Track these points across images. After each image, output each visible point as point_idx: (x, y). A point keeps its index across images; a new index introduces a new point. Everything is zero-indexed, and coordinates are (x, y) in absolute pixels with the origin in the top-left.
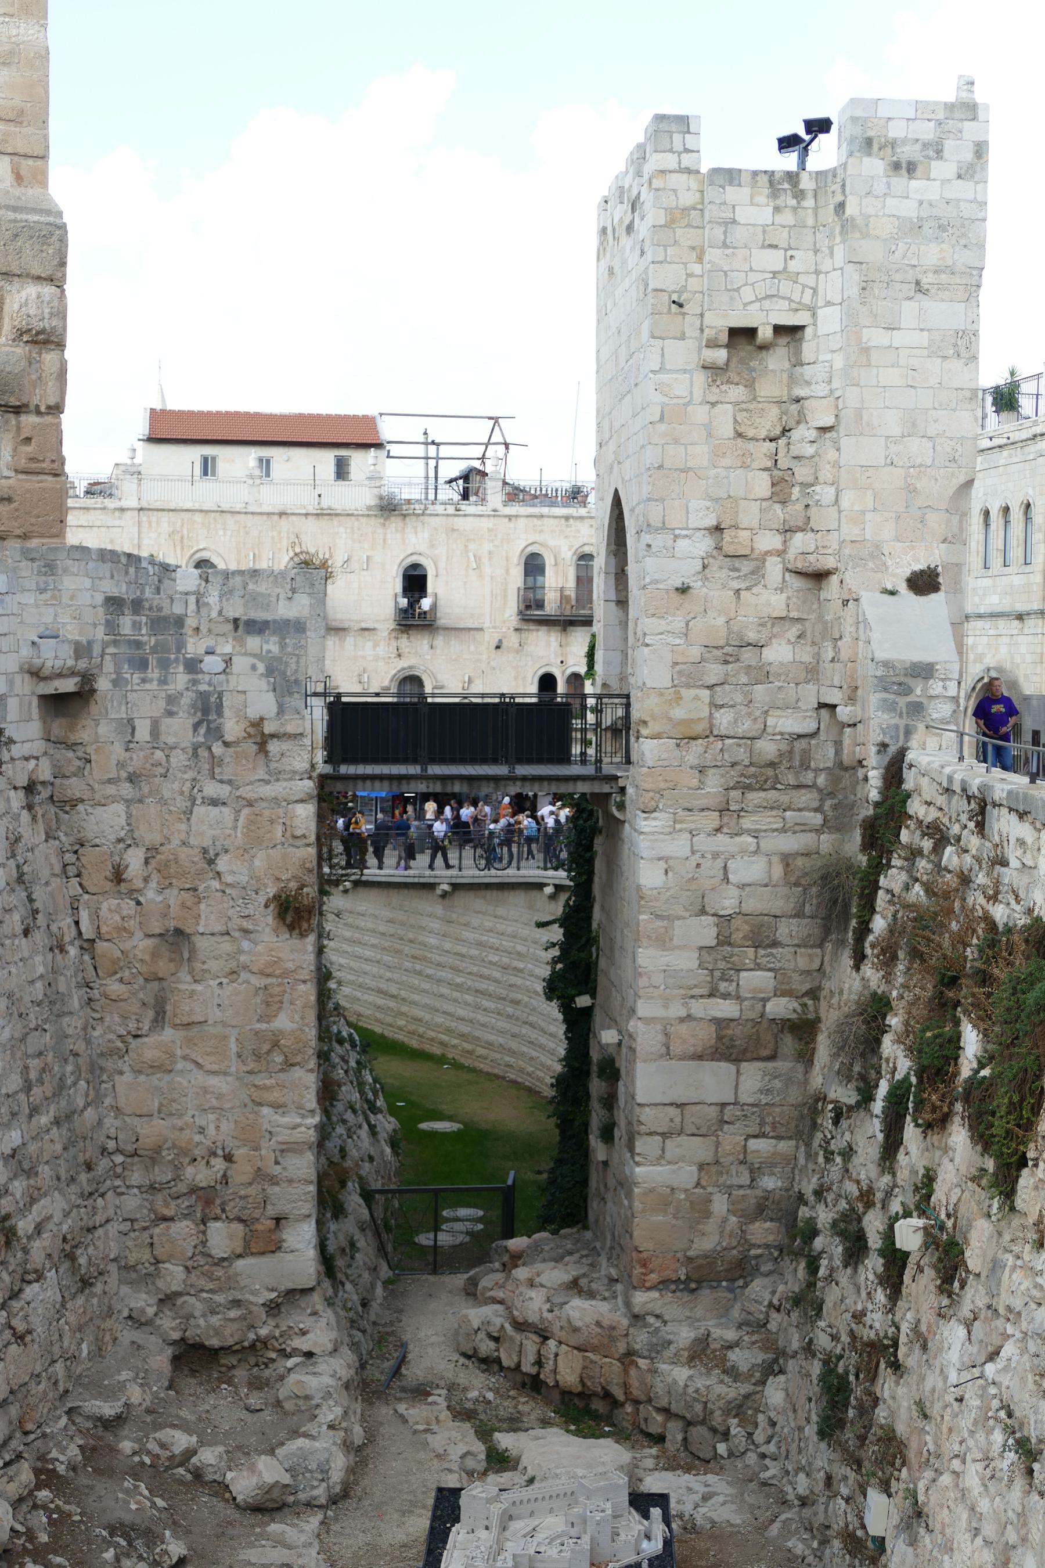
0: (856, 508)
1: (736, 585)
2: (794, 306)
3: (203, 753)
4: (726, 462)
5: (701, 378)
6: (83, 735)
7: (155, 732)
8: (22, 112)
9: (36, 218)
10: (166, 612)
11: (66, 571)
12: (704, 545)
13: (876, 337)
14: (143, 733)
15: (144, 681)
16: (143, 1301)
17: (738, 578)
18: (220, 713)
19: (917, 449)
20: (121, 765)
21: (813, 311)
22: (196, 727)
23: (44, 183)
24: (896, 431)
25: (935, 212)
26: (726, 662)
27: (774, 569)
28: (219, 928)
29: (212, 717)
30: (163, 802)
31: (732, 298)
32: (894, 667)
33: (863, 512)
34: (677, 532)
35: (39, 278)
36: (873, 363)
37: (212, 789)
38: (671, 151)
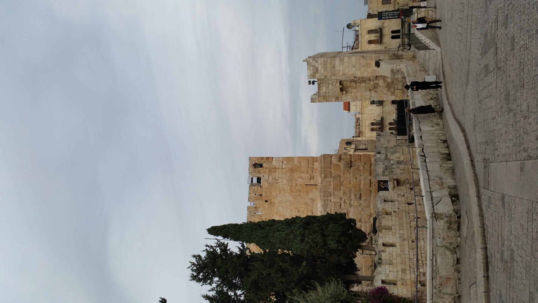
3: (405, 163)
4: (360, 90)
5: (348, 94)
6: (403, 180)
7: (402, 170)
8: (307, 161)
9: (322, 159)
10: (384, 168)
11: (378, 173)
12: (372, 92)
13: (341, 73)
15: (395, 171)
18: (399, 161)
19: (357, 66)
21: (337, 80)
22: (401, 164)
23: (317, 157)
24: (355, 69)
25: (323, 66)
26: (391, 88)
27: (376, 82)
29: (400, 162)
31: (336, 92)
32: (392, 75)
33: (367, 73)
35: (331, 158)
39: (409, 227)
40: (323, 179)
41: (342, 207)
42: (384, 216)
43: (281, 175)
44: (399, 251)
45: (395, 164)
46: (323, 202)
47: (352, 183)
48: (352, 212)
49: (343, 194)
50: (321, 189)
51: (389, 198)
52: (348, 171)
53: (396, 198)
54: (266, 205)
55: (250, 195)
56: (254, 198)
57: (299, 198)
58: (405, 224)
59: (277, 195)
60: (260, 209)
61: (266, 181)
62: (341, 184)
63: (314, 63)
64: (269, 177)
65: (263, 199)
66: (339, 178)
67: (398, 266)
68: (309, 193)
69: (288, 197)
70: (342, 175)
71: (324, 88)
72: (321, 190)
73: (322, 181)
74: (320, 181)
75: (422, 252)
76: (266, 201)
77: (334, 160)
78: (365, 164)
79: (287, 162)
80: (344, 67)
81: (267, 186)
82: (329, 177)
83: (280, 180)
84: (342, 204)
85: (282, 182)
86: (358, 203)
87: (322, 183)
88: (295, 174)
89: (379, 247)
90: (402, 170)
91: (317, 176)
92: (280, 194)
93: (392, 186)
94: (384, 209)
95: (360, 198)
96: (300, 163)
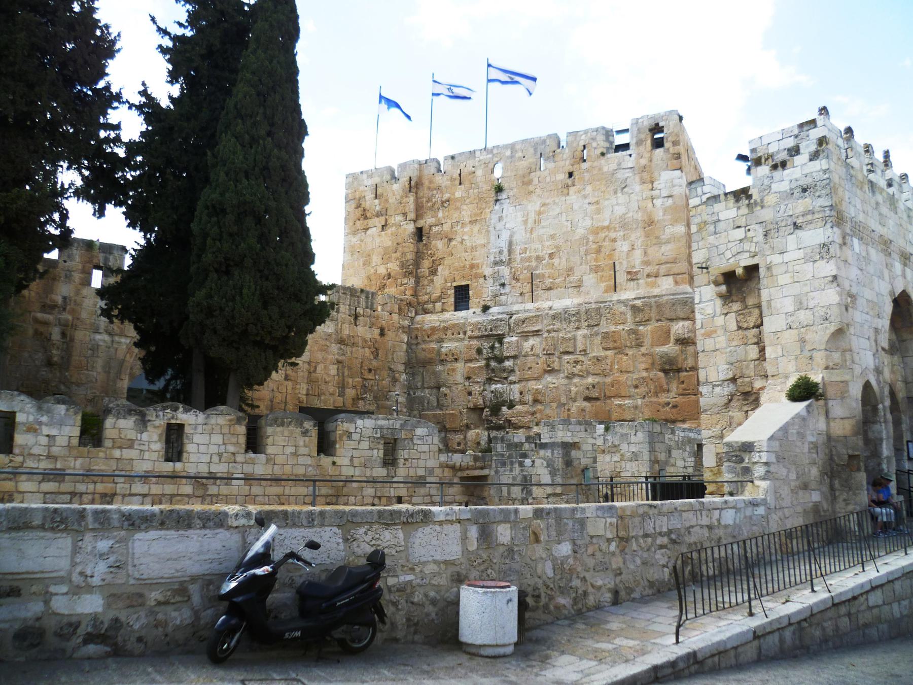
0: (772, 357)
1: (745, 408)
2: (752, 254)
15: (505, 471)
17: (747, 404)
19: (804, 316)
24: (791, 309)
25: (799, 183)
31: (721, 259)
34: (714, 383)
36: (774, 274)
38: (697, 196)
40: (631, 303)
41: (566, 358)
43: (636, 198)
44: (143, 467)
45: (522, 471)
46: (573, 310)
47: (625, 376)
48: (554, 381)
49: (594, 357)
50: (606, 302)
51: (402, 454)
52: (653, 364)
53: (402, 472)
54: (562, 176)
55: (581, 133)
56: (575, 145)
57: (582, 253)
59: (585, 197)
60: (551, 165)
61: (619, 164)
62: (619, 350)
63: (808, 146)
64: (628, 170)
65: (575, 167)
66: (633, 343)
67: (75, 460)
68: (595, 275)
69: (584, 224)
70: (643, 350)
71: (732, 213)
72: (601, 302)
73: (624, 303)
76: (571, 175)
77: (679, 328)
78: (675, 406)
79: (670, 207)
80: (797, 268)
81: (605, 169)
82: (635, 318)
84: (571, 357)
85: (617, 204)
86: (576, 393)
87: (620, 302)
88: (640, 233)
89: (161, 413)
91: (638, 289)
92: (589, 203)
93: (458, 464)
95: (587, 399)
96: (668, 242)
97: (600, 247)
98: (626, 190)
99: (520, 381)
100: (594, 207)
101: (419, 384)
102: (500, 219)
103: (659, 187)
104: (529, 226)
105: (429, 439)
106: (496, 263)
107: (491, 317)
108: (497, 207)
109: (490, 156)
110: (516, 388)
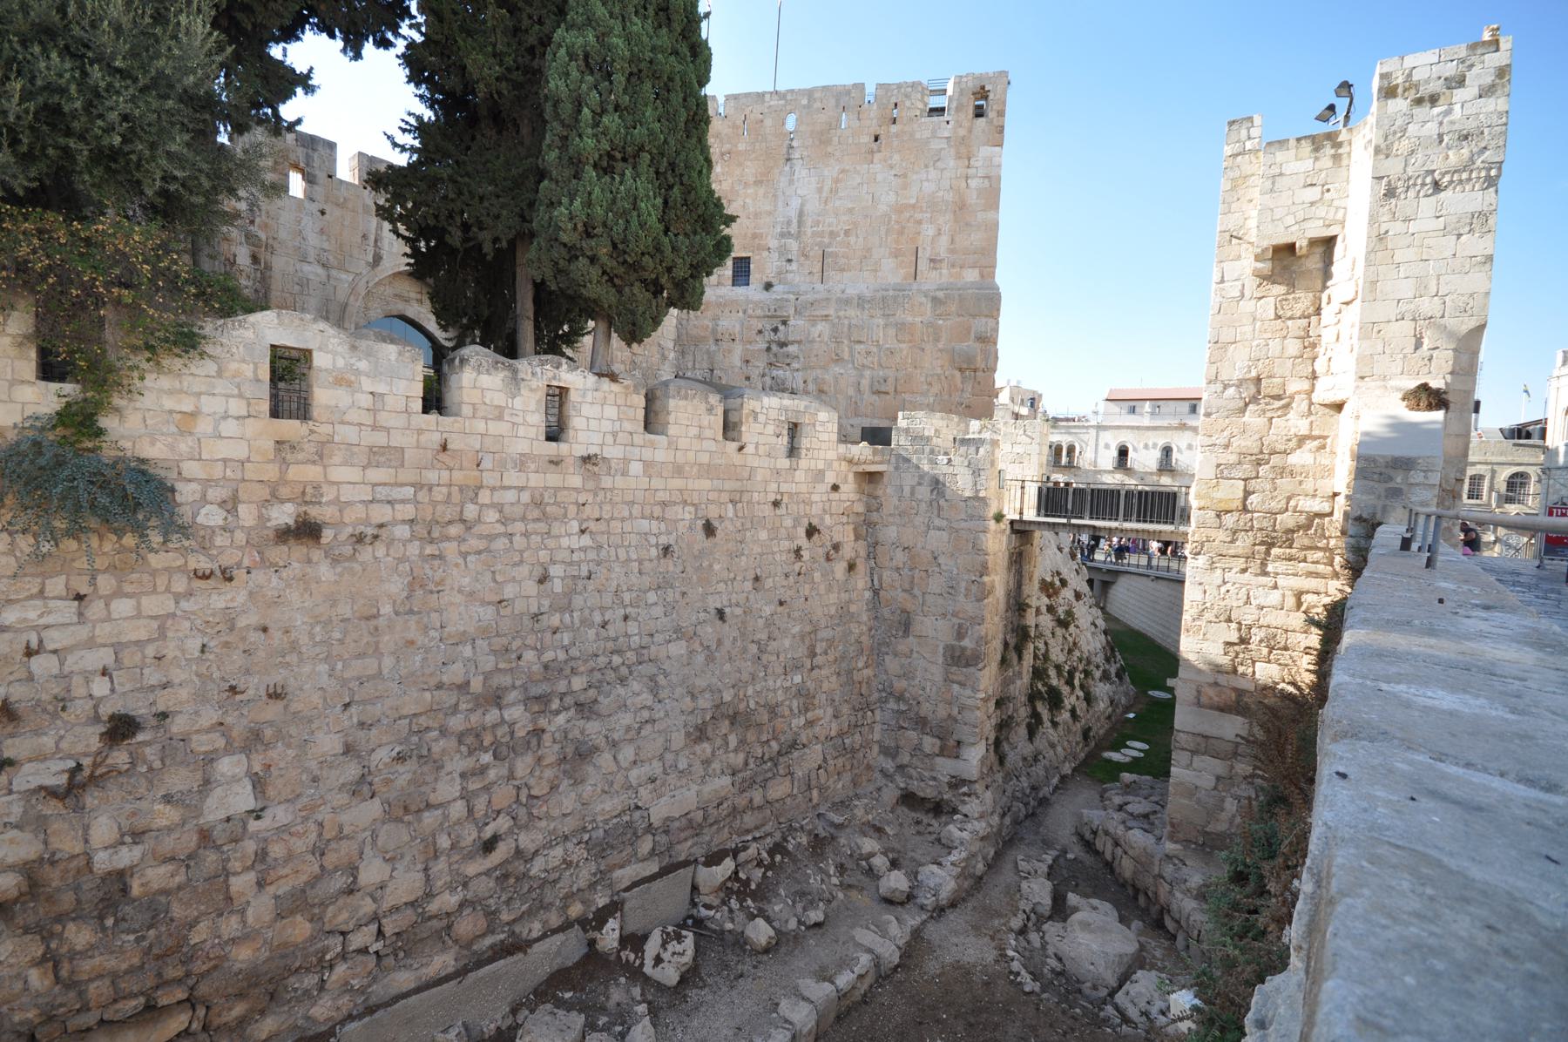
6: (880, 493)
7: (912, 493)
14: (907, 490)
16: (889, 765)
20: (896, 508)
22: (932, 491)
28: (938, 591)
30: (915, 527)
32: (1374, 461)
37: (937, 522)
39: (661, 496)
41: (858, 347)
42: (720, 410)
51: (804, 442)
53: (803, 463)
54: (867, 139)
57: (883, 233)
58: (677, 483)
61: (934, 131)
69: (887, 199)
74: (924, 288)
75: (517, 538)
76: (876, 139)
81: (918, 136)
83: (933, 174)
85: (928, 180)
88: (949, 216)
90: (912, 493)
94: (756, 419)
97: (903, 228)
98: (938, 164)
99: (805, 369)
100: (900, 180)
101: (690, 366)
102: (791, 182)
103: (977, 164)
104: (824, 195)
105: (830, 425)
106: (783, 235)
107: (774, 296)
108: (787, 168)
109: (782, 102)
110: (799, 376)
